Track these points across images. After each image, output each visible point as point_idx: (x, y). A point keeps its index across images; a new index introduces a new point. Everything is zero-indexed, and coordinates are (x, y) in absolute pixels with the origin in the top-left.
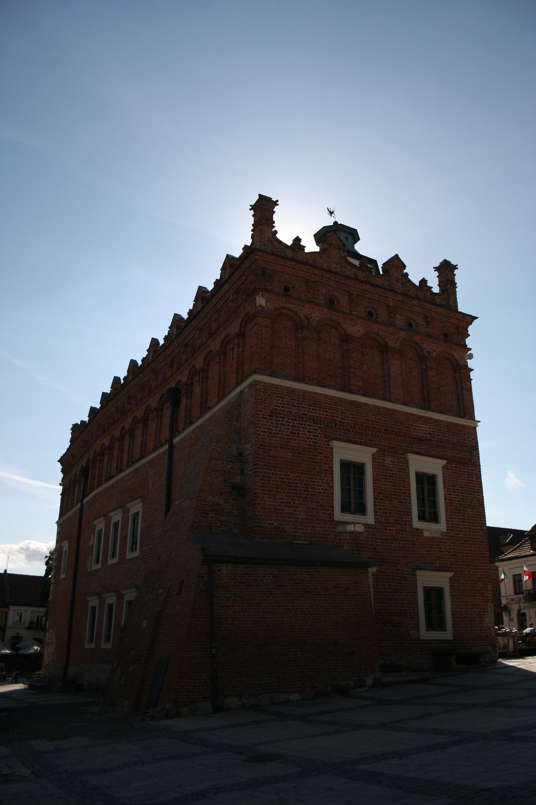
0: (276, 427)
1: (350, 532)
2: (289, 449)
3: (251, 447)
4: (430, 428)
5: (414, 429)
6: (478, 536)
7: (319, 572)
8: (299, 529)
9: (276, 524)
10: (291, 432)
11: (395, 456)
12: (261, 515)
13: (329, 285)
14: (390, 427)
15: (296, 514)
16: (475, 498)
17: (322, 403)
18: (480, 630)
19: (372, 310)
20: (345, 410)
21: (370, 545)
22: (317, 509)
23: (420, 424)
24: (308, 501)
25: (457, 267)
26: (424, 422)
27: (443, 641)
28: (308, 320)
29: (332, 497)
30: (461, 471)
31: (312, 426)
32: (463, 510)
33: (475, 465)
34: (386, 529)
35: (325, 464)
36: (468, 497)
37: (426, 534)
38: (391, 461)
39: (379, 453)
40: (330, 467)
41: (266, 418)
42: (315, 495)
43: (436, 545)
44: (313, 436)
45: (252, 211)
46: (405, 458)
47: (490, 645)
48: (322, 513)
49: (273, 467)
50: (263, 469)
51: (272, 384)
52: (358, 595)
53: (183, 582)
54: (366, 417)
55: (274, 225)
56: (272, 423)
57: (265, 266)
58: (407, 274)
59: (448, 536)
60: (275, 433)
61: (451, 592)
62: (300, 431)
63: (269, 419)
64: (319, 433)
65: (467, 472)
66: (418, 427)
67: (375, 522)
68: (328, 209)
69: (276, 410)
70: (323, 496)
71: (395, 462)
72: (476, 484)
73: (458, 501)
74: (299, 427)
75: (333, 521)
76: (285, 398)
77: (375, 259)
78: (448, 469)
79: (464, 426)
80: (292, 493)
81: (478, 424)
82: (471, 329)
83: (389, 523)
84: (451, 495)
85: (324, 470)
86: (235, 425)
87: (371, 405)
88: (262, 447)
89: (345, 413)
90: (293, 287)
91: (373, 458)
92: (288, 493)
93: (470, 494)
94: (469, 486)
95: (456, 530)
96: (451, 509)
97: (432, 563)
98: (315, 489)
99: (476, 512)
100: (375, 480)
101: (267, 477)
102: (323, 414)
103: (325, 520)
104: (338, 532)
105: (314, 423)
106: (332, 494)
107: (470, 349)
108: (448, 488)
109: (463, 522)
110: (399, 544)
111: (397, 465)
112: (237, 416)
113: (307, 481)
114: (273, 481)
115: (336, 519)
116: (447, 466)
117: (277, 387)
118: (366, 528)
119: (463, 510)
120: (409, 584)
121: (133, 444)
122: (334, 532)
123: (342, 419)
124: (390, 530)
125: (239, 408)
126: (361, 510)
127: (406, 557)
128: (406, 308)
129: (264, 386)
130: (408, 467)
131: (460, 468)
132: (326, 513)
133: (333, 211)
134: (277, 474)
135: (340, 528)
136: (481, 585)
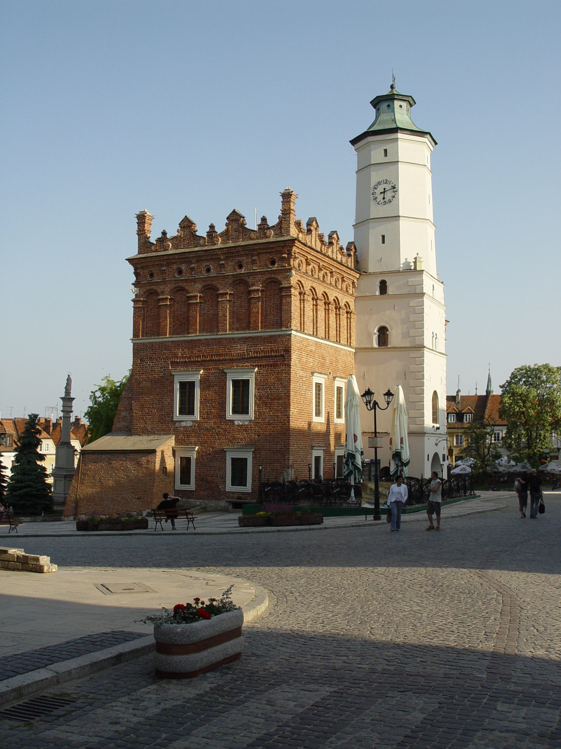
5: (235, 349)
12: (135, 422)
26: (243, 341)
35: (169, 386)
36: (276, 392)
37: (236, 423)
38: (214, 376)
42: (164, 407)
46: (224, 372)
48: (167, 417)
49: (141, 393)
51: (141, 343)
59: (255, 423)
60: (142, 373)
61: (253, 461)
69: (143, 358)
70: (168, 406)
78: (260, 374)
85: (169, 390)
87: (203, 340)
98: (163, 403)
102: (170, 355)
103: (169, 421)
106: (173, 404)
108: (258, 388)
110: (215, 431)
111: (218, 378)
115: (174, 420)
118: (193, 423)
130: (226, 378)
132: (169, 417)
134: (143, 397)
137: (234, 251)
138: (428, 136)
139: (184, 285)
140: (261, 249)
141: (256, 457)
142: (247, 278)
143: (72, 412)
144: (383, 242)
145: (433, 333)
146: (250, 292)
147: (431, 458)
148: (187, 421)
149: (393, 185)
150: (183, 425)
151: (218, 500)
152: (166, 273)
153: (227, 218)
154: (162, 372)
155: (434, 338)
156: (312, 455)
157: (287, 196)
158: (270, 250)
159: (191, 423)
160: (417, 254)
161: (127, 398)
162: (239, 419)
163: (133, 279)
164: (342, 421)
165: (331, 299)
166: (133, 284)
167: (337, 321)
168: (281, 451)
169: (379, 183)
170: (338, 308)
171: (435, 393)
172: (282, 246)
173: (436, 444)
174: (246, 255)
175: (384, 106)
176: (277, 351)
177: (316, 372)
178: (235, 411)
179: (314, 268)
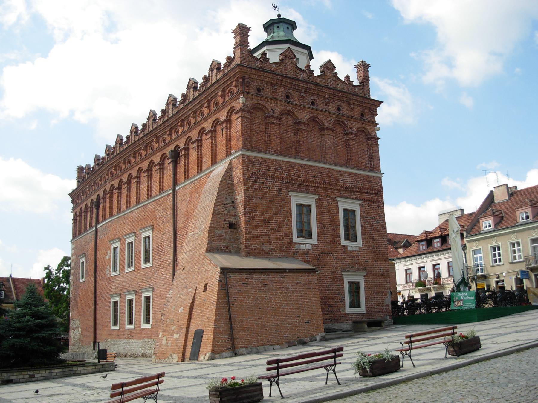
0: (256, 184)
1: (302, 250)
2: (264, 198)
3: (240, 198)
4: (352, 180)
5: (342, 181)
6: (382, 248)
7: (288, 275)
8: (272, 249)
9: (258, 247)
10: (265, 188)
11: (330, 200)
13: (286, 86)
14: (326, 181)
15: (270, 240)
16: (381, 224)
17: (284, 167)
18: (382, 307)
19: (314, 101)
20: (298, 171)
21: (315, 257)
22: (282, 236)
23: (346, 177)
24: (277, 231)
25: (370, 65)
26: (348, 176)
27: (359, 315)
29: (291, 228)
30: (372, 207)
31: (278, 182)
32: (372, 233)
33: (380, 203)
34: (325, 247)
35: (286, 207)
36: (376, 224)
37: (349, 249)
38: (328, 203)
39: (320, 198)
40: (289, 209)
41: (249, 179)
43: (356, 255)
44: (279, 189)
45: (233, 34)
46: (336, 200)
47: (388, 316)
48: (286, 238)
50: (249, 212)
51: (252, 156)
52: (311, 288)
53: (206, 285)
54: (311, 174)
55: (249, 45)
56: (253, 182)
57: (244, 75)
58: (336, 74)
59: (363, 250)
60: (255, 189)
61: (365, 284)
62: (271, 186)
63: (251, 179)
64: (282, 187)
65: (375, 208)
66: (344, 179)
67: (318, 242)
68: (273, 5)
69: (255, 173)
71: (330, 203)
72: (381, 215)
73: (370, 227)
74: (270, 184)
75: (292, 243)
76: (260, 165)
77: (309, 45)
78: (363, 206)
79: (374, 177)
80: (267, 226)
81: (383, 175)
82: (379, 110)
83: (327, 243)
84: (365, 223)
85: (286, 211)
86: (228, 183)
88: (248, 198)
89: (298, 173)
90: (263, 89)
91: (316, 202)
92: (264, 226)
93: (377, 222)
94: (377, 217)
95: (368, 246)
96: (365, 232)
97: (353, 267)
98: (281, 223)
99: (381, 233)
101: (251, 217)
102: (285, 175)
104: (296, 250)
105: (279, 180)
106: (291, 226)
107: (378, 124)
108: (363, 219)
109: (372, 240)
110: (333, 256)
112: (229, 177)
113: (276, 218)
114: (255, 219)
115: (294, 242)
116: (363, 204)
117: (255, 158)
118: (312, 246)
119: (372, 233)
120: (339, 280)
121: (139, 187)
122: (293, 249)
123: (296, 177)
124: (327, 247)
125: (230, 171)
127: (338, 264)
128: (336, 98)
129: (247, 158)
130: (338, 206)
131: (371, 205)
132: (287, 238)
133: (277, 6)
134: (257, 215)
135: (297, 247)
136: (383, 280)
137: (338, 94)
139: (293, 110)
141: (366, 281)
148: (307, 244)
150: (301, 248)
151: (339, 323)
152: (276, 92)
154: (278, 191)
158: (362, 104)
159: (311, 246)
161: (222, 214)
162: (352, 246)
168: (384, 275)
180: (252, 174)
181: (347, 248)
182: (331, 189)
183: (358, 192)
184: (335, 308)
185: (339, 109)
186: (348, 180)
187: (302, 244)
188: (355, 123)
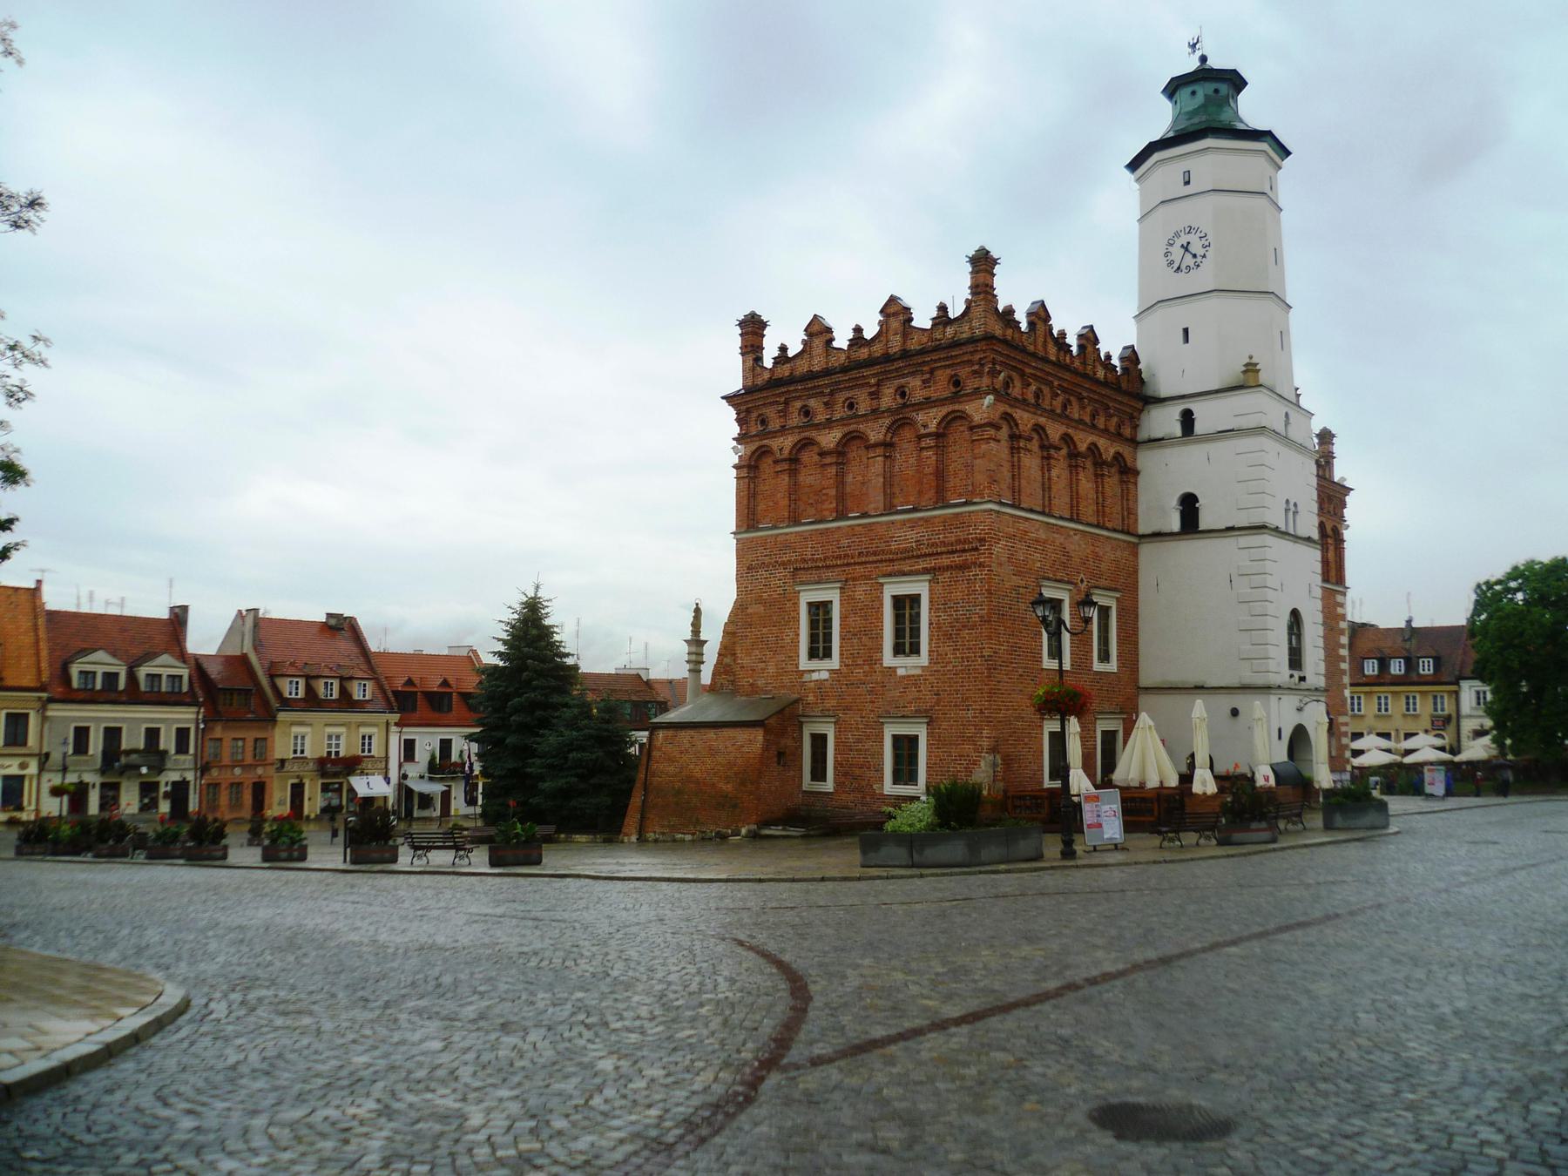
28: (781, 450)
51: (747, 539)
79: (970, 512)
100: (843, 618)
117: (752, 540)
126: (827, 654)
130: (882, 593)
135: (806, 677)
138: (1269, 139)
139: (813, 434)
140: (935, 361)
142: (914, 414)
143: (703, 663)
144: (1186, 340)
145: (1287, 502)
146: (920, 437)
147: (1286, 735)
148: (821, 670)
149: (1203, 235)
153: (881, 312)
155: (1291, 515)
156: (1042, 730)
157: (983, 263)
160: (1251, 357)
162: (907, 666)
163: (735, 430)
164: (1113, 666)
165: (1083, 447)
166: (734, 439)
167: (1097, 487)
169: (1177, 235)
170: (1099, 463)
171: (1295, 614)
172: (971, 352)
173: (1300, 709)
174: (913, 374)
175: (1184, 93)
176: (966, 541)
177: (1048, 579)
178: (898, 650)
179: (1042, 392)
180: (748, 568)
181: (895, 672)
182: (876, 562)
183: (930, 555)
184: (864, 783)
185: (903, 395)
186: (912, 535)
187: (813, 671)
188: (935, 410)
